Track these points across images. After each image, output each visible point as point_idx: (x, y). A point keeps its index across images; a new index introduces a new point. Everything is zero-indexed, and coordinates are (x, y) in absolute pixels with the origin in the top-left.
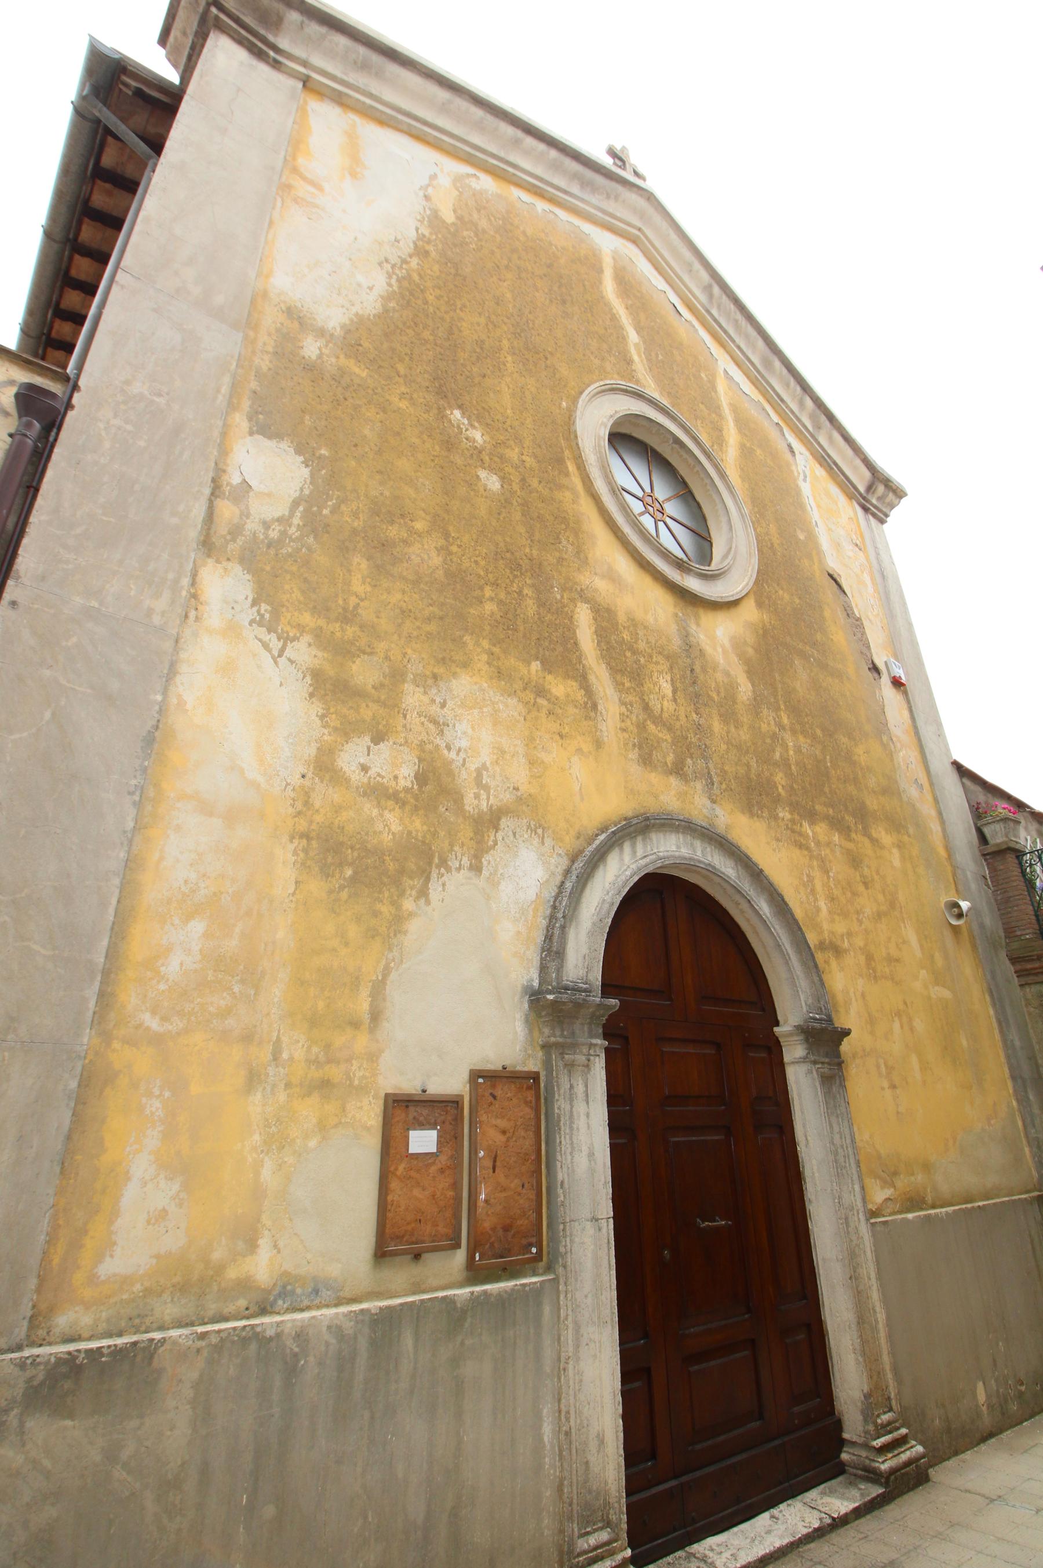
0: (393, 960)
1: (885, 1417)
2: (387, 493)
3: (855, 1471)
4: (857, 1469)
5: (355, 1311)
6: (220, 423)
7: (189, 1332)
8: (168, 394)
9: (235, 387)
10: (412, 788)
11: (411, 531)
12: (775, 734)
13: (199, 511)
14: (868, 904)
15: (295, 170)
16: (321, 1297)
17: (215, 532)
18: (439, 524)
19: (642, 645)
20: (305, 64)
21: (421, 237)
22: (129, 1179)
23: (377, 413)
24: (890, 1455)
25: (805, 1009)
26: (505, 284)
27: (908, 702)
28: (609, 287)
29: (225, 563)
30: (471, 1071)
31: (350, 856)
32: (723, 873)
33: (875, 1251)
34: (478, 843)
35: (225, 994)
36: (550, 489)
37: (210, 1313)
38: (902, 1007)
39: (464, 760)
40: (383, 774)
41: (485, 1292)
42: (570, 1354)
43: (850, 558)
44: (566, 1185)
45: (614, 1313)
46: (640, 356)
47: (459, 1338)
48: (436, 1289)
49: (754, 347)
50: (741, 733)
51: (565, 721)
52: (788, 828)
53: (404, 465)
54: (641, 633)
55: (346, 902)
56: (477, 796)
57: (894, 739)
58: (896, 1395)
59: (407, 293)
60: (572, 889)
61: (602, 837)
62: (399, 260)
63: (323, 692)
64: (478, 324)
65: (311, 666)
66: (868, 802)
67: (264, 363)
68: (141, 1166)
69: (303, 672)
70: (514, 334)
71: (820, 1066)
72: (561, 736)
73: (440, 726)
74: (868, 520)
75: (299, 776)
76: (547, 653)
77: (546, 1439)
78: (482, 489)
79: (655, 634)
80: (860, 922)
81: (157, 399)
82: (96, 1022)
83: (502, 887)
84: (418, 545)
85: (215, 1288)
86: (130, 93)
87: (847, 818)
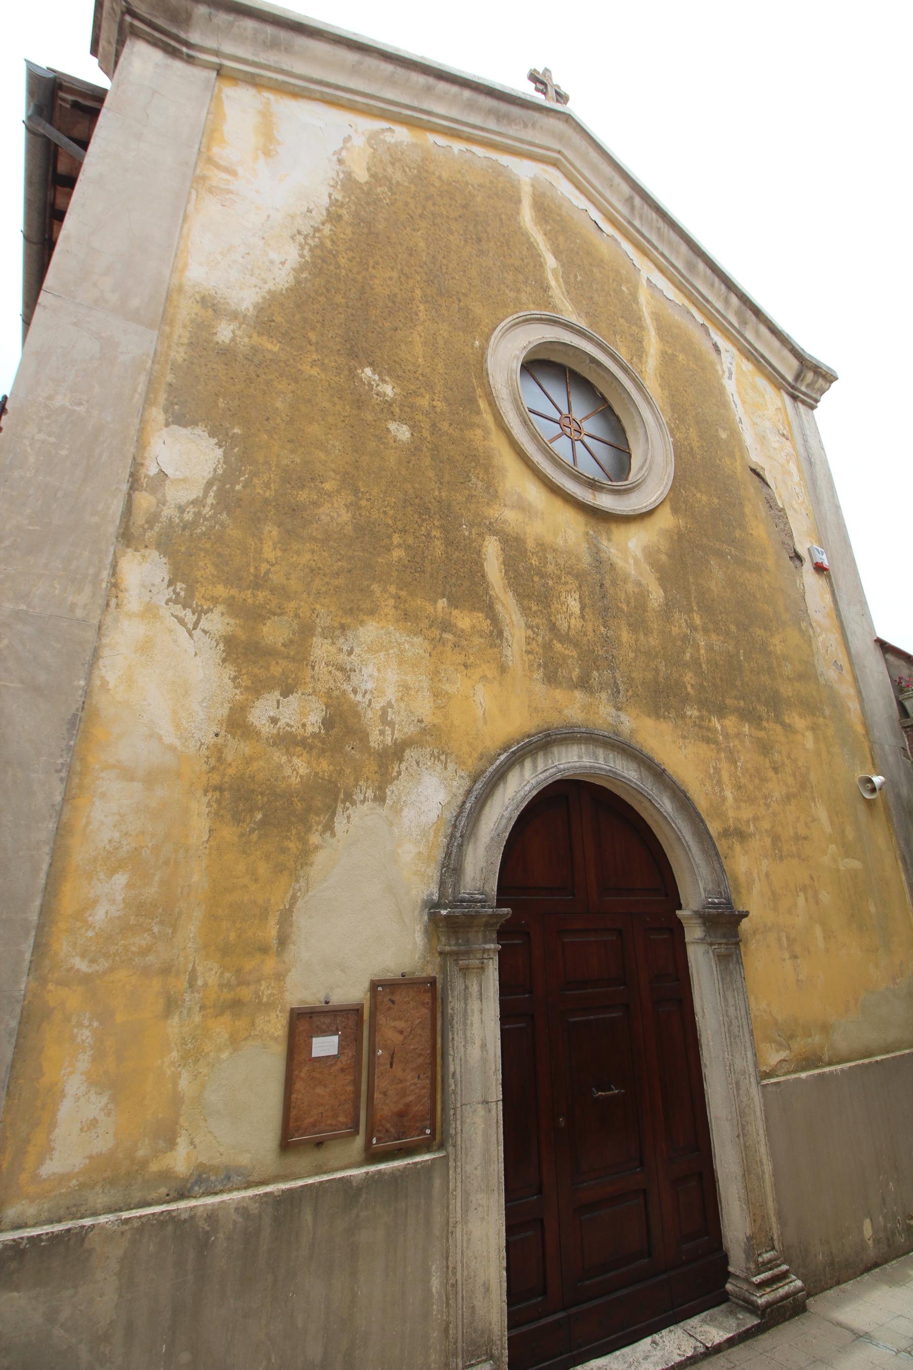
1: (767, 1256)
2: (298, 460)
4: (740, 1299)
5: (260, 1195)
6: (137, 421)
7: (115, 1218)
8: (87, 402)
12: (686, 635)
13: (117, 506)
14: (776, 788)
15: (210, 161)
16: (232, 1182)
17: (134, 523)
19: (551, 568)
20: (217, 53)
21: (334, 203)
22: (64, 1096)
23: (289, 385)
24: (768, 1290)
25: (703, 895)
26: (419, 233)
27: (831, 585)
28: (527, 216)
29: (142, 551)
31: (260, 802)
32: (624, 777)
34: (382, 775)
35: (146, 935)
36: (461, 430)
37: (136, 1200)
39: (370, 701)
40: (292, 723)
41: (379, 1171)
42: (458, 1219)
43: (775, 449)
46: (557, 281)
49: (677, 252)
50: (651, 639)
51: (470, 652)
52: (695, 725)
53: (315, 430)
54: (550, 557)
55: (256, 843)
56: (382, 733)
57: (814, 624)
58: (779, 1237)
59: (320, 262)
60: (471, 810)
61: (502, 758)
62: (312, 229)
63: (234, 656)
64: (391, 279)
65: (224, 634)
66: (782, 690)
67: (179, 355)
68: (74, 1085)
71: (716, 947)
72: (466, 666)
73: (346, 672)
74: (796, 409)
77: (434, 1290)
78: (392, 441)
79: (565, 556)
80: (768, 806)
81: (77, 409)
83: (405, 813)
86: (68, 106)
87: (759, 707)
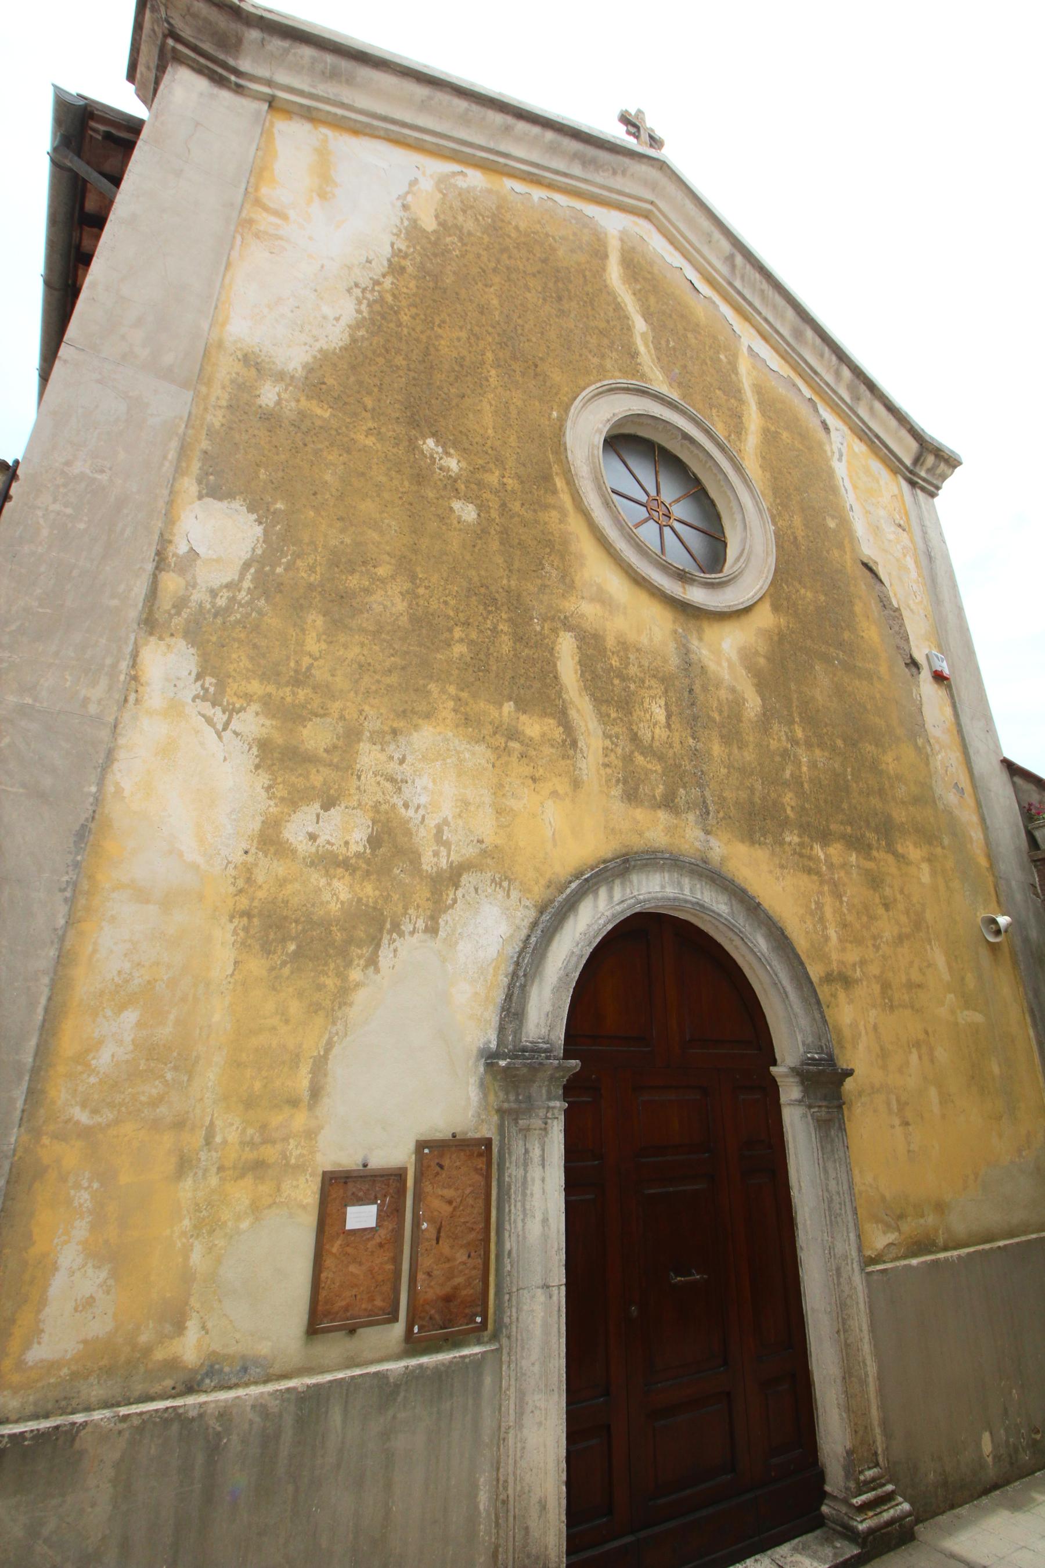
0: (337, 1034)
1: (869, 1474)
2: (348, 540)
3: (834, 1526)
4: (837, 1524)
5: (281, 1390)
6: (166, 492)
7: (112, 1415)
8: (110, 469)
9: (184, 451)
10: (365, 852)
11: (374, 579)
12: (786, 750)
13: (140, 588)
14: (887, 928)
15: (258, 202)
16: (250, 1375)
17: (159, 608)
18: (405, 566)
19: (633, 670)
20: (269, 83)
21: (397, 253)
22: (56, 1269)
23: (340, 455)
24: (871, 1514)
25: (801, 1050)
26: (492, 289)
27: (952, 697)
28: (614, 273)
29: (168, 639)
30: (417, 1141)
31: (294, 930)
32: (713, 911)
33: (869, 1302)
34: (434, 903)
35: (157, 1083)
36: (535, 511)
37: (137, 1394)
38: (922, 1036)
39: (423, 817)
40: (333, 841)
41: (421, 1366)
42: (511, 1424)
43: (890, 541)
44: (514, 1254)
45: (561, 1381)
46: (647, 346)
47: (390, 1413)
48: (372, 1362)
49: (782, 317)
50: (746, 754)
51: (540, 763)
52: (795, 853)
53: (368, 507)
54: (632, 657)
55: (288, 978)
56: (436, 854)
57: (932, 741)
58: (883, 1451)
59: (379, 318)
60: (536, 945)
61: (573, 886)
62: (371, 282)
63: (269, 762)
64: (459, 339)
65: (259, 736)
66: (895, 814)
67: (216, 419)
68: (69, 1256)
69: (249, 744)
70: (500, 344)
71: (816, 1110)
72: (534, 780)
73: (397, 783)
74: (915, 496)
75: (241, 852)
76: (522, 691)
77: (482, 1507)
78: (455, 522)
79: (649, 656)
80: (877, 948)
81: (99, 476)
82: (25, 1119)
83: (460, 946)
84: (380, 592)
85: (142, 1369)
86: (100, 138)
87: (867, 834)
